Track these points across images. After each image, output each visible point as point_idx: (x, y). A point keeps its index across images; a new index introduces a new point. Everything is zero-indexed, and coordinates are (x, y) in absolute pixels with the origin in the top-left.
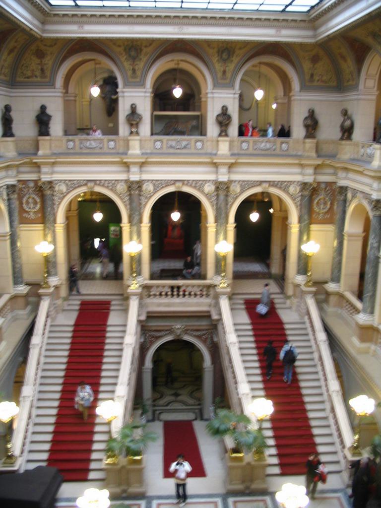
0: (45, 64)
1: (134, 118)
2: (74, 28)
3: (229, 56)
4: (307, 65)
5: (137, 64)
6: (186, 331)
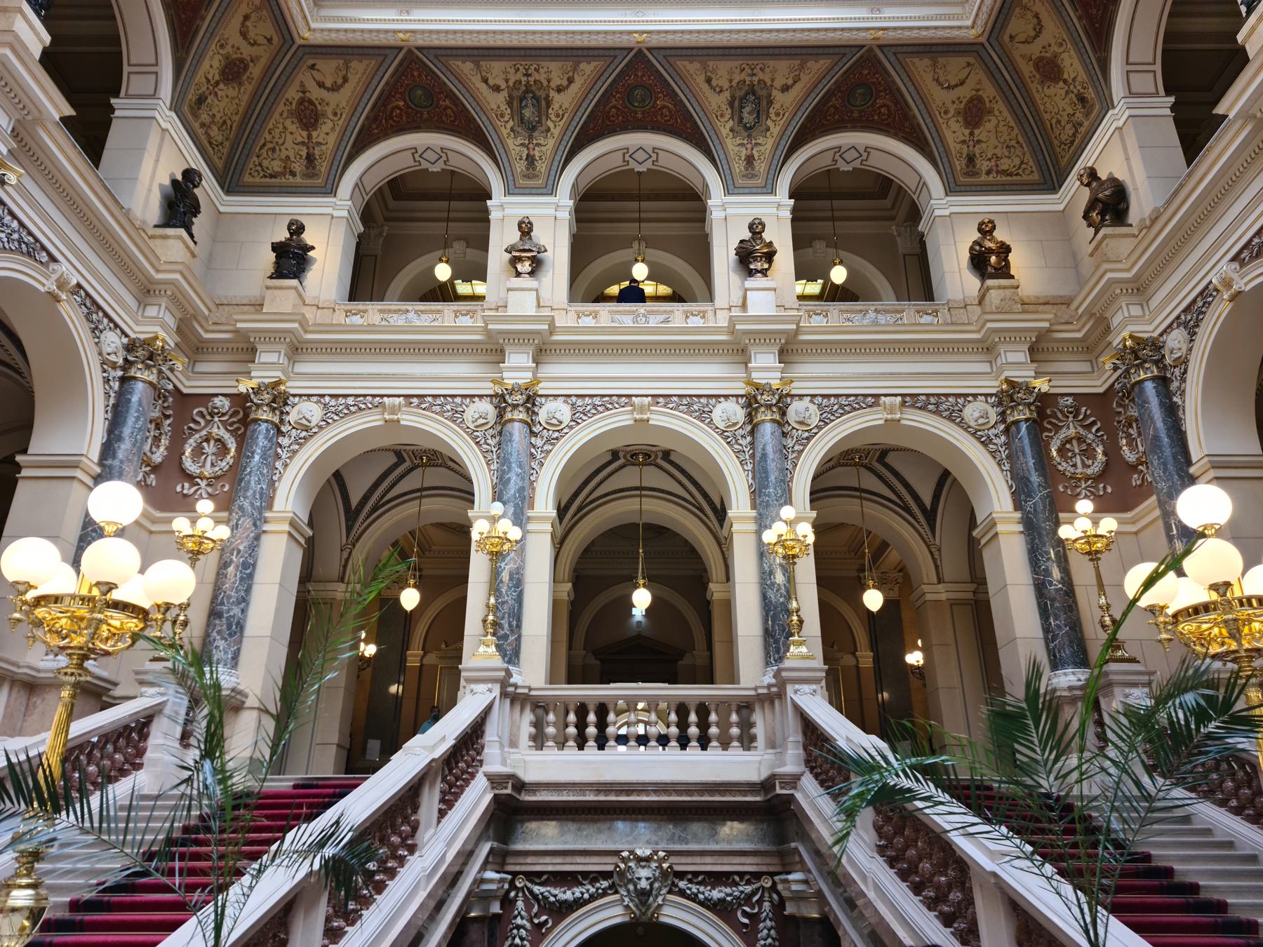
0: (319, 144)
1: (528, 258)
2: (390, 14)
3: (758, 117)
4: (954, 132)
5: (538, 145)
6: (671, 878)
